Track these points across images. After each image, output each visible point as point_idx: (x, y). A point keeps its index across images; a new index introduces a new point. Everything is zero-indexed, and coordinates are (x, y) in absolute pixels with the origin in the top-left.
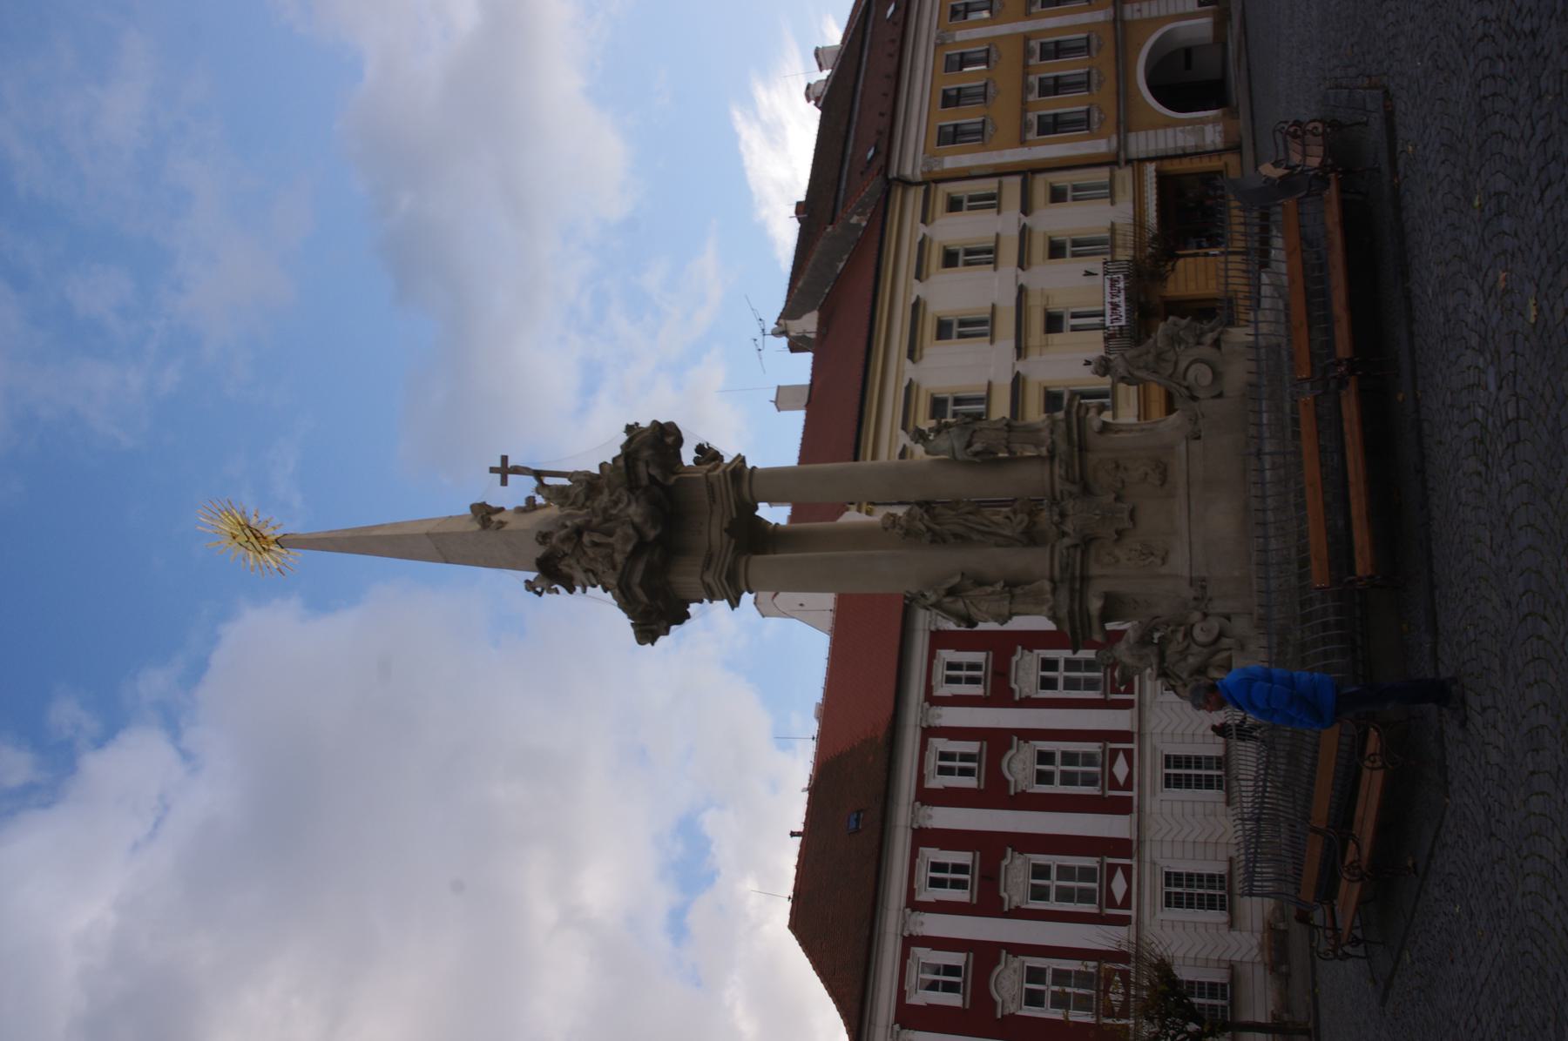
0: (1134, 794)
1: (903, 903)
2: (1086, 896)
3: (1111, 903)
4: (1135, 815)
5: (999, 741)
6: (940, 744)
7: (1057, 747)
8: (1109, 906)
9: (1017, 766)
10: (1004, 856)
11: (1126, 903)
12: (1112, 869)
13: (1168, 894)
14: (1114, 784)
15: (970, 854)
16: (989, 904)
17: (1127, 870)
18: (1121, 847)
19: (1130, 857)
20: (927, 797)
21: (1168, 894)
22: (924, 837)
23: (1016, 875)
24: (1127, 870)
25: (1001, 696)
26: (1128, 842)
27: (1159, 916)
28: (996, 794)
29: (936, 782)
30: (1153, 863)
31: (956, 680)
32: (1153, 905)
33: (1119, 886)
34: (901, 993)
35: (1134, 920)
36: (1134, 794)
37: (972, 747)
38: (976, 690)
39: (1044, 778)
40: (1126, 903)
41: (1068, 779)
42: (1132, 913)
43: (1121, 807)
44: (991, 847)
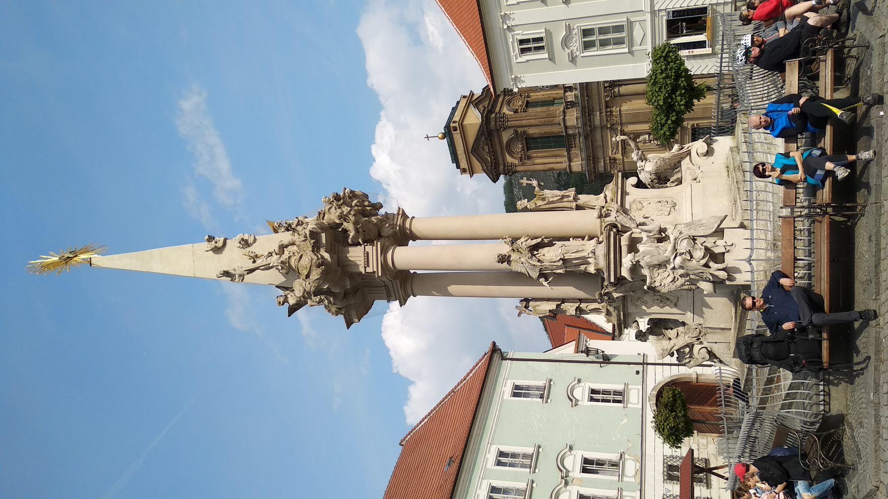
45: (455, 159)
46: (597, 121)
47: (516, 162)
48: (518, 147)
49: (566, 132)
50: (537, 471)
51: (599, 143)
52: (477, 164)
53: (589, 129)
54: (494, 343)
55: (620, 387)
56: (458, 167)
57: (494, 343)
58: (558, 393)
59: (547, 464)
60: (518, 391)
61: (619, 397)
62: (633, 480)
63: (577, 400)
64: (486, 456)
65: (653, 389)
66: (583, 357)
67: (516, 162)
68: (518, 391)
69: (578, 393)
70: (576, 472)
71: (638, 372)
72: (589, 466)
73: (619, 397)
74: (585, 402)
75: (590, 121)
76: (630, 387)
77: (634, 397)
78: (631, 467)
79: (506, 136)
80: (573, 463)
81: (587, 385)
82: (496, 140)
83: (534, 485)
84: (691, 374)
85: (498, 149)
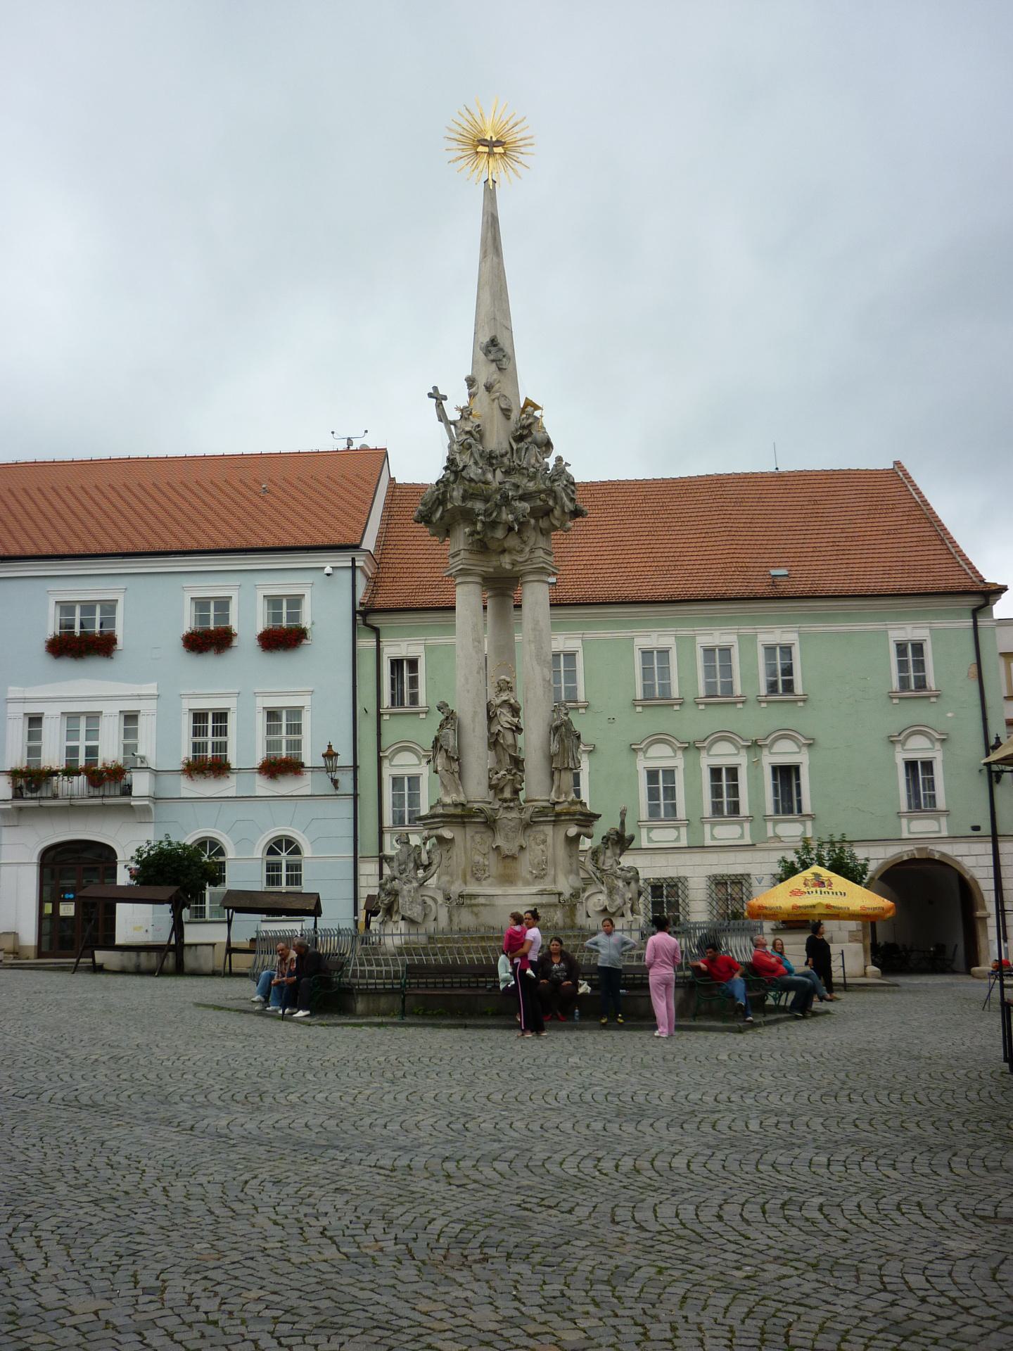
50: (764, 705)
54: (1004, 589)
55: (941, 803)
57: (1004, 589)
58: (918, 713)
59: (776, 717)
60: (911, 654)
62: (770, 834)
63: (903, 743)
64: (777, 632)
65: (944, 855)
66: (993, 742)
68: (911, 654)
70: (769, 759)
71: (976, 828)
72: (786, 775)
74: (900, 757)
76: (943, 820)
77: (922, 827)
80: (785, 753)
81: (937, 756)
83: (740, 706)
84: (984, 908)
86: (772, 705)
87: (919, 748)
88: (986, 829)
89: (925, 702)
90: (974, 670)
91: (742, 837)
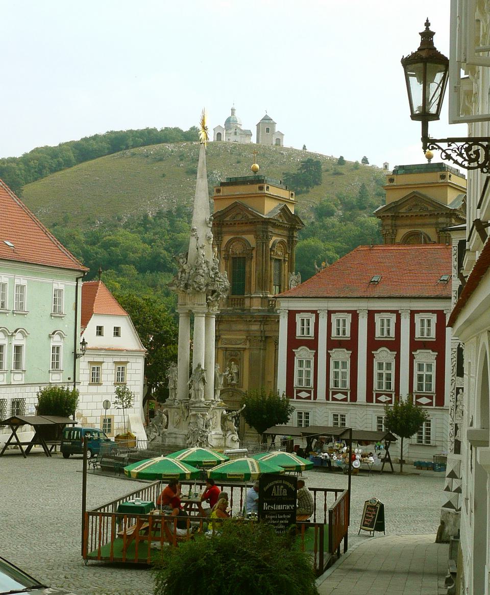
0: (374, 404)
1: (330, 309)
2: (336, 384)
3: (334, 393)
4: (365, 404)
5: (394, 345)
6: (393, 318)
7: (393, 372)
8: (332, 392)
9: (384, 354)
10: (347, 350)
11: (334, 399)
12: (346, 394)
13: (337, 415)
14: (378, 395)
15: (349, 336)
16: (332, 344)
17: (345, 400)
18: (354, 398)
19: (351, 401)
20: (371, 314)
21: (337, 415)
22: (355, 315)
23: (342, 355)
24: (345, 400)
25: (415, 345)
26: (355, 400)
27: (330, 412)
28: (373, 345)
29: (377, 318)
30: (348, 410)
31: (423, 325)
32: (333, 409)
33: (339, 396)
34: (299, 312)
35: (328, 402)
36: (374, 404)
37: (392, 334)
38: (418, 334)
39: (380, 365)
40: (334, 399)
41: (380, 375)
42: (330, 401)
43: (369, 398)
44: (351, 345)
45: (232, 182)
46: (255, 327)
47: (223, 245)
48: (237, 249)
49: (247, 297)
51: (234, 327)
52: (223, 206)
53: (248, 320)
56: (222, 184)
61: (56, 365)
67: (223, 245)
69: (56, 337)
71: (69, 379)
73: (56, 365)
75: (255, 321)
78: (18, 378)
79: (250, 238)
80: (18, 340)
82: (245, 228)
85: (236, 228)
86: (18, 315)
87: (56, 341)
88: (72, 380)
89: (61, 318)
90: (75, 306)
91: (3, 381)
